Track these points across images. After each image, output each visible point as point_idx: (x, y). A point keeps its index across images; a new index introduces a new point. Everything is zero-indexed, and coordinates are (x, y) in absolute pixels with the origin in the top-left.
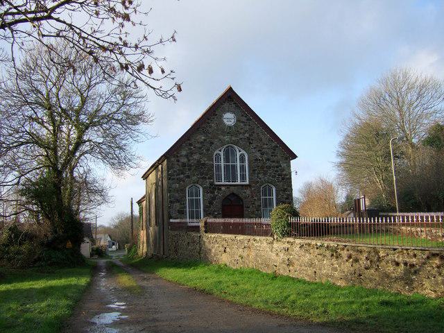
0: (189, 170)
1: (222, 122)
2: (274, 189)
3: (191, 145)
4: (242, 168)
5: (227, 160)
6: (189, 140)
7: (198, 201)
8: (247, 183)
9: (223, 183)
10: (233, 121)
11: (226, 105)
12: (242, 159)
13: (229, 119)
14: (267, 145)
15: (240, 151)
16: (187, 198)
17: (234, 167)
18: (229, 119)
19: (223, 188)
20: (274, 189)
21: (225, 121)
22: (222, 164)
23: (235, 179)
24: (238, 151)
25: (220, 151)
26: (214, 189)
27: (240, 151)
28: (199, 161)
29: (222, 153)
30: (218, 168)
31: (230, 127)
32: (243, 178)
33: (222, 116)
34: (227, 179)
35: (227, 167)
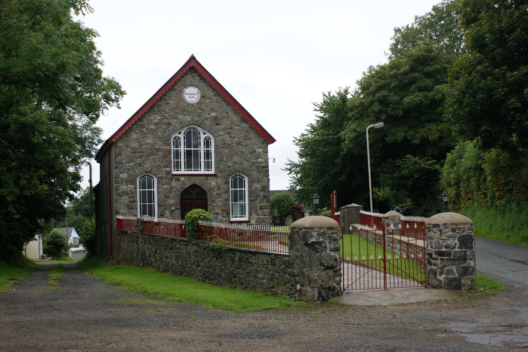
0: (141, 157)
2: (246, 179)
3: (142, 126)
4: (208, 155)
7: (151, 194)
8: (212, 172)
9: (183, 171)
11: (189, 78)
12: (207, 143)
13: (192, 94)
14: (238, 126)
15: (204, 134)
16: (138, 190)
17: (197, 153)
18: (192, 94)
19: (182, 179)
20: (246, 179)
21: (187, 97)
22: (182, 149)
24: (202, 134)
25: (180, 133)
26: (171, 179)
27: (204, 134)
28: (153, 146)
29: (182, 136)
30: (177, 154)
31: (192, 105)
32: (208, 166)
33: (182, 92)
34: (188, 166)
35: (188, 154)
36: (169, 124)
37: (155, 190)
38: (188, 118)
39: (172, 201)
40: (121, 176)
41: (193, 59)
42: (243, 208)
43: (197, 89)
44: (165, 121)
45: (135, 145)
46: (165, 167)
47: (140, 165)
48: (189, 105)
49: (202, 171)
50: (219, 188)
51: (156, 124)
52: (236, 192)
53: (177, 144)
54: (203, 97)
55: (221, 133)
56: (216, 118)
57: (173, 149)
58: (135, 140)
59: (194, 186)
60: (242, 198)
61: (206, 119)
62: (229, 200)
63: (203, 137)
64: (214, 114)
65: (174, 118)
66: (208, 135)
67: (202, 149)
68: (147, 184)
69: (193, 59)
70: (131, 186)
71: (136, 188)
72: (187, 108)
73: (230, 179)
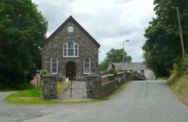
0: (52, 51)
1: (67, 31)
2: (90, 59)
3: (53, 40)
4: (76, 50)
5: (69, 47)
6: (52, 38)
7: (55, 64)
8: (78, 57)
9: (67, 56)
10: (72, 30)
11: (69, 23)
12: (76, 47)
13: (71, 29)
17: (72, 50)
18: (71, 29)
19: (67, 59)
20: (90, 59)
21: (69, 30)
22: (67, 49)
23: (72, 55)
24: (74, 43)
25: (66, 43)
26: (63, 59)
28: (56, 47)
29: (67, 44)
30: (65, 50)
31: (71, 33)
32: (76, 54)
34: (69, 55)
35: (69, 50)
36: (62, 40)
37: (57, 63)
38: (69, 38)
39: (63, 67)
40: (45, 58)
41: (71, 16)
42: (89, 69)
43: (73, 27)
44: (61, 39)
45: (50, 47)
46: (60, 55)
47: (52, 54)
49: (74, 56)
50: (80, 62)
51: (58, 40)
53: (65, 47)
54: (75, 30)
55: (81, 43)
56: (79, 38)
57: (63, 49)
58: (50, 45)
59: (71, 62)
60: (88, 66)
61: (76, 38)
62: (83, 67)
63: (74, 44)
65: (64, 38)
66: (76, 43)
67: (74, 49)
68: (54, 61)
69: (71, 16)
70: (48, 61)
71: (50, 62)
72: (68, 34)
73: (84, 60)
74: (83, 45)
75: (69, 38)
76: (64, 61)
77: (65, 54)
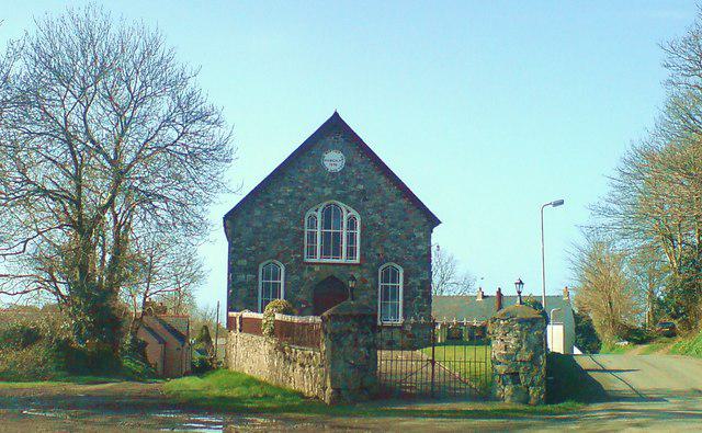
0: (265, 239)
3: (269, 200)
4: (351, 238)
5: (327, 225)
8: (358, 261)
9: (317, 260)
10: (339, 164)
11: (330, 140)
12: (352, 224)
13: (334, 160)
14: (392, 202)
17: (338, 236)
18: (334, 160)
19: (317, 268)
20: (401, 272)
21: (327, 164)
23: (337, 253)
24: (345, 212)
25: (316, 211)
27: (349, 212)
29: (319, 215)
30: (312, 235)
32: (351, 253)
33: (320, 157)
34: (326, 253)
35: (326, 237)
36: (303, 199)
37: (282, 281)
38: (328, 191)
42: (395, 307)
47: (263, 249)
48: (333, 174)
49: (343, 260)
50: (365, 282)
51: (286, 198)
52: (387, 287)
53: (313, 224)
54: (349, 164)
59: (332, 280)
60: (395, 296)
64: (361, 187)
65: (311, 191)
66: (353, 212)
73: (380, 271)
74: (377, 218)
75: (328, 191)
76: (306, 274)
77: (312, 253)
